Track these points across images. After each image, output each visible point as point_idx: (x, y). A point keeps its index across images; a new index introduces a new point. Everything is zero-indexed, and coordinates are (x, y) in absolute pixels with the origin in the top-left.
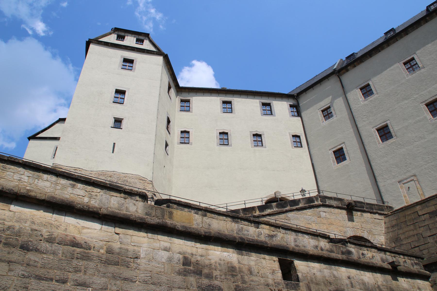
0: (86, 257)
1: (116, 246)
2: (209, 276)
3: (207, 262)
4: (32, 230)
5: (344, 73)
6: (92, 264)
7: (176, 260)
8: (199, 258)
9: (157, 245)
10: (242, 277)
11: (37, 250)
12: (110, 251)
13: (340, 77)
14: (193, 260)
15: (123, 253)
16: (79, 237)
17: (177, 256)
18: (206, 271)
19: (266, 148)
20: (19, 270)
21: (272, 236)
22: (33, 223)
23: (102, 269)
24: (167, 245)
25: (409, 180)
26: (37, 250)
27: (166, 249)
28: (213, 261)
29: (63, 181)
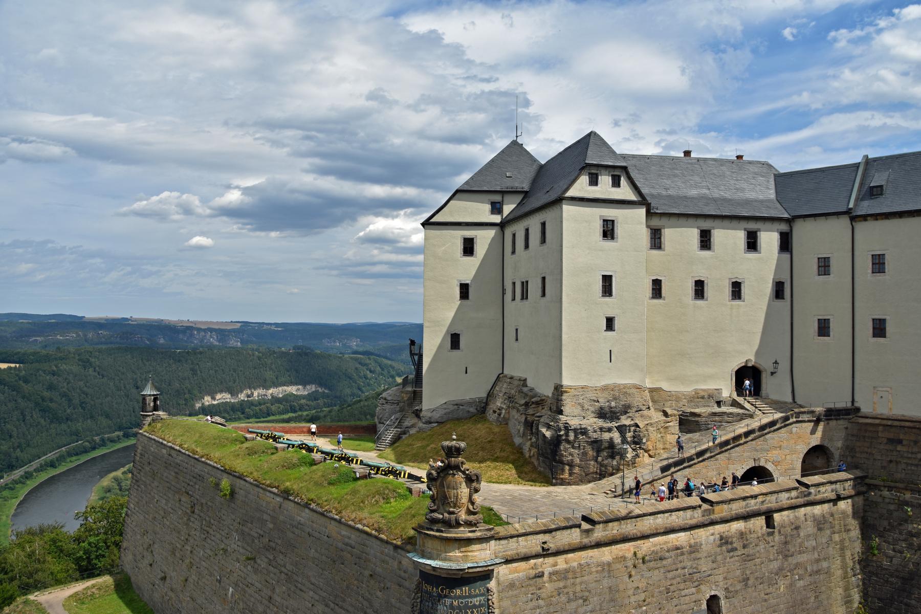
0: (682, 554)
1: (692, 541)
2: (731, 543)
3: (730, 534)
4: (661, 548)
5: (860, 221)
6: (685, 557)
7: (717, 539)
11: (665, 558)
12: (690, 546)
13: (853, 223)
14: (724, 536)
18: (730, 540)
19: (744, 301)
20: (662, 570)
22: (660, 544)
24: (712, 531)
25: (884, 389)
26: (665, 558)
27: (713, 534)
29: (666, 515)
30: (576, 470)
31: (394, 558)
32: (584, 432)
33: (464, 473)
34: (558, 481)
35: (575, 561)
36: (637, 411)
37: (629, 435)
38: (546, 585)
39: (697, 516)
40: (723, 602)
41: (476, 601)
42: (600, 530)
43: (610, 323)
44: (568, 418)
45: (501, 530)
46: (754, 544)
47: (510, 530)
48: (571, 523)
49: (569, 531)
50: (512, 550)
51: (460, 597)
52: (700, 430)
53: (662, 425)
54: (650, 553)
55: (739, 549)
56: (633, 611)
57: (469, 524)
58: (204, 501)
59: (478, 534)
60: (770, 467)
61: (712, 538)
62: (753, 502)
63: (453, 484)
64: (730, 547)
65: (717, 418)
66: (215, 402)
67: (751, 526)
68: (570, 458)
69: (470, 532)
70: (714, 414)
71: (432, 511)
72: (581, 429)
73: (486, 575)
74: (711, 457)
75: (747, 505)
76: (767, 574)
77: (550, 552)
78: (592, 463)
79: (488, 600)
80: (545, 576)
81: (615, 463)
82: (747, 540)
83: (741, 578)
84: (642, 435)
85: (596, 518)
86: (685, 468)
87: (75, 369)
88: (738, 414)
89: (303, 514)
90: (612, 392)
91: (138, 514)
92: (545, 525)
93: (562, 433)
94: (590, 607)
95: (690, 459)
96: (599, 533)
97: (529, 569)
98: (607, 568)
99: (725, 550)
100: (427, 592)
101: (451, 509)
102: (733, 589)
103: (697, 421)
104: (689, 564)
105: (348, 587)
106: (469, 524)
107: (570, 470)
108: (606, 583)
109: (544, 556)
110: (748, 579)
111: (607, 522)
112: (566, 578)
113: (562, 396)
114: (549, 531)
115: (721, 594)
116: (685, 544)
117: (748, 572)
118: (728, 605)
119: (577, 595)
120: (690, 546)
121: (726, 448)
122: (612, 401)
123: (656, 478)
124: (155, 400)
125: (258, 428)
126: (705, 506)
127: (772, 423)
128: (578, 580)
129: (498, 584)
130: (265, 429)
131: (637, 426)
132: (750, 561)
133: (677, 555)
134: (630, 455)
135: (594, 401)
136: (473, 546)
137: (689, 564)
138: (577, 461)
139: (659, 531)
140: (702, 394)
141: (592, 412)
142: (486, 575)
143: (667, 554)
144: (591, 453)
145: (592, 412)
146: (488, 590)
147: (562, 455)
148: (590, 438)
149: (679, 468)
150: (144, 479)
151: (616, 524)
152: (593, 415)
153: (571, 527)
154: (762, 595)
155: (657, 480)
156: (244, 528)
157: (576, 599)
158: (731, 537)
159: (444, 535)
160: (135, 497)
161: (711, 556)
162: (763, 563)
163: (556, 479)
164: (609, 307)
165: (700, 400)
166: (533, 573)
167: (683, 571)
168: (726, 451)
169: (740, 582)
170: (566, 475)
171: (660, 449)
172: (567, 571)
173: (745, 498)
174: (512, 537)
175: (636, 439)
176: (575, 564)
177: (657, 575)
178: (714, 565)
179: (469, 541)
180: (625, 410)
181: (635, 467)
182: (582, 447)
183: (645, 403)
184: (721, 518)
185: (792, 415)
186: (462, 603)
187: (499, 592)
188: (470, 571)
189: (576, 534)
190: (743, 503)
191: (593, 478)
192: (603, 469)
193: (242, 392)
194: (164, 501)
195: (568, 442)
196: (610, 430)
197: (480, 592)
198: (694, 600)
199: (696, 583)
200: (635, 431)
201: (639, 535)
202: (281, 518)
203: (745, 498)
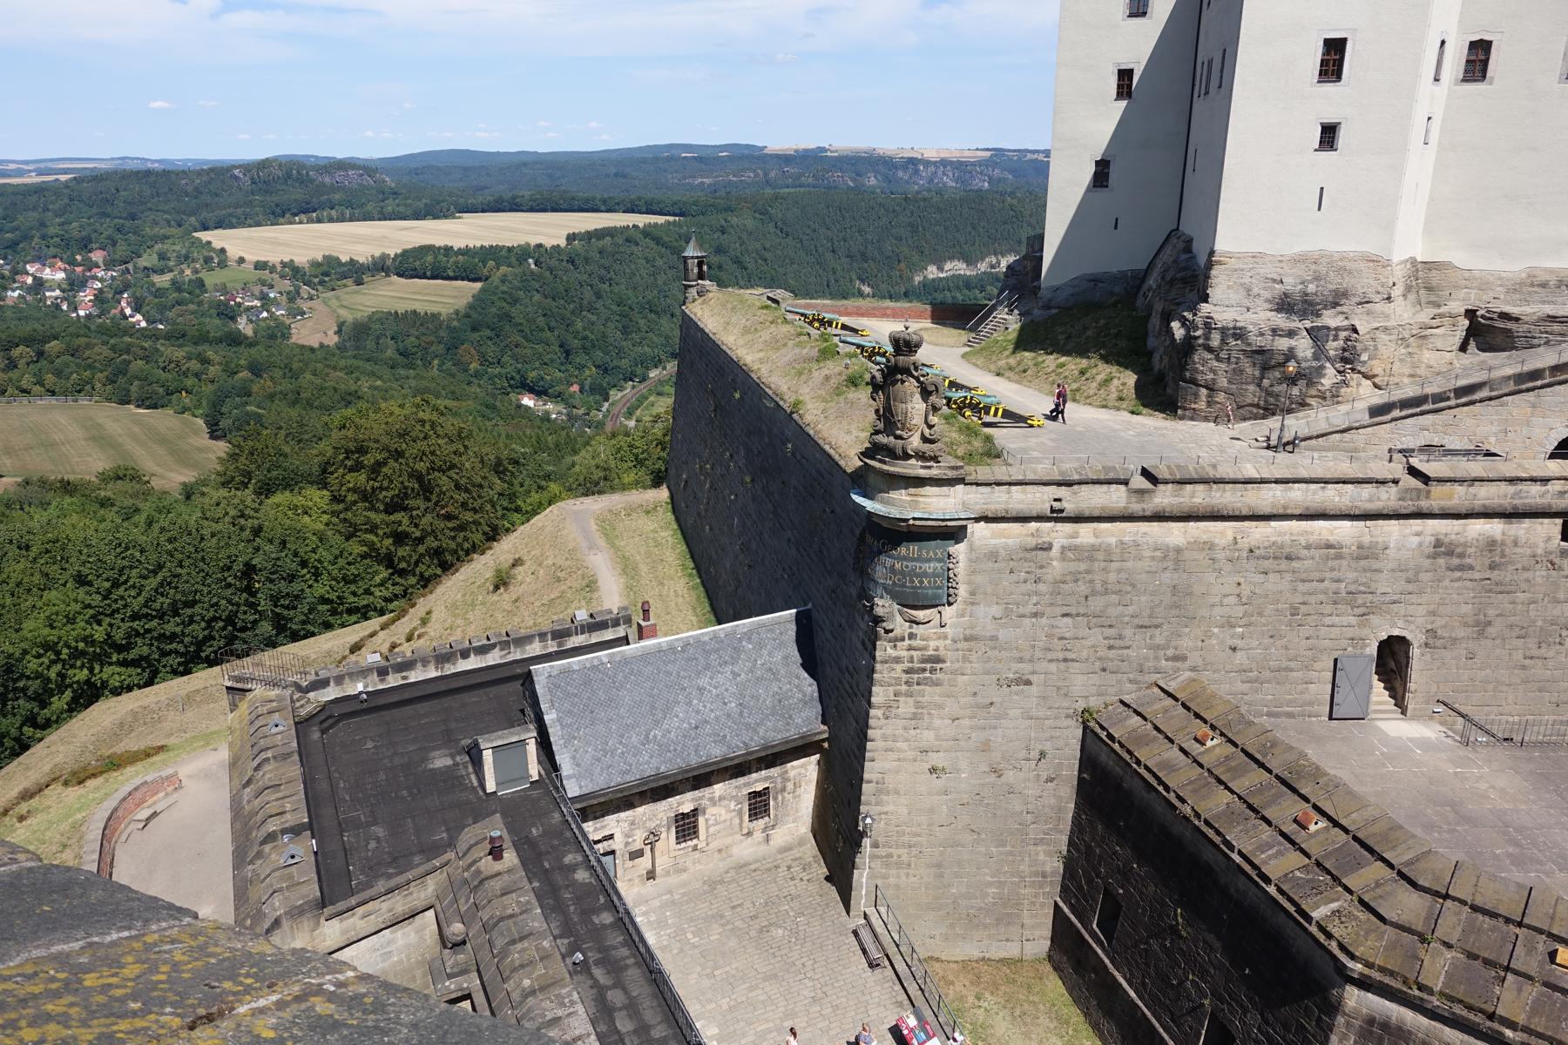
0: (1339, 557)
1: (1366, 540)
3: (1462, 540)
6: (1345, 563)
8: (1453, 537)
9: (1407, 531)
10: (1502, 551)
12: (1360, 547)
15: (1373, 545)
17: (1429, 540)
18: (1459, 550)
23: (1353, 564)
24: (1419, 529)
26: (1298, 558)
27: (1418, 534)
28: (1469, 539)
29: (1313, 486)
30: (1220, 397)
32: (1239, 333)
33: (917, 379)
34: (1188, 413)
35: (1113, 535)
36: (1360, 303)
37: (1333, 347)
38: (1055, 563)
39: (1387, 498)
40: (1415, 652)
41: (930, 567)
42: (1168, 493)
43: (1329, 135)
44: (1217, 308)
45: (999, 471)
46: (1519, 566)
47: (999, 471)
48: (1111, 475)
49: (1105, 487)
50: (998, 503)
51: (905, 558)
52: (1516, 348)
53: (1415, 332)
54: (1266, 544)
55: (1478, 568)
56: (1216, 630)
57: (921, 456)
59: (935, 472)
61: (1416, 540)
62: (1536, 489)
63: (901, 394)
64: (1456, 561)
65: (1556, 327)
66: (941, 275)
67: (1523, 532)
68: (1211, 376)
69: (922, 467)
71: (877, 432)
72: (1235, 328)
73: (954, 533)
74: (1490, 399)
75: (1515, 494)
76: (1540, 623)
77: (1064, 515)
78: (1252, 388)
79: (949, 569)
80: (1054, 550)
81: (1295, 391)
82: (1503, 555)
83: (1470, 620)
84: (1359, 346)
85: (1162, 472)
86: (1422, 413)
87: (750, 223)
90: (1313, 267)
92: (1062, 473)
93: (1198, 333)
94: (1131, 610)
96: (1164, 498)
97: (1027, 535)
98: (1174, 557)
99: (1443, 566)
101: (898, 432)
102: (1445, 635)
103: (1510, 330)
104: (1351, 576)
106: (921, 456)
107: (1209, 396)
108: (1167, 577)
109: (1057, 520)
110: (1489, 623)
112: (1091, 559)
114: (1069, 484)
115: (1415, 637)
116: (1347, 541)
117: (1491, 612)
118: (1428, 657)
119: (1109, 586)
120: (1360, 547)
121: (1531, 385)
122: (1310, 282)
123: (1357, 425)
124: (700, 264)
125: (801, 306)
126: (1414, 483)
129: (971, 549)
130: (807, 306)
131: (1355, 331)
132: (1501, 593)
134: (1329, 378)
135: (1274, 281)
136: (928, 488)
137: (1351, 576)
138: (1223, 382)
139: (1289, 512)
140: (1543, 277)
141: (1267, 301)
142: (954, 533)
143: (1305, 552)
144: (1250, 371)
145: (1267, 301)
146: (949, 556)
147: (1196, 371)
148: (1249, 344)
149: (1410, 411)
151: (1200, 487)
153: (1109, 482)
154: (1518, 656)
155: (1357, 428)
157: (1106, 592)
158: (1465, 545)
159: (885, 467)
161: (1407, 570)
162: (1534, 602)
163: (1185, 409)
164: (1331, 102)
165: (1536, 289)
166: (1032, 542)
167: (1335, 585)
168: (1528, 390)
169: (1466, 625)
170: (1202, 405)
171: (1402, 375)
172: (1095, 548)
173: (1512, 481)
174: (999, 484)
175: (1346, 354)
177: (1274, 583)
178: (1410, 587)
179: (920, 482)
180: (1336, 300)
181: (1338, 403)
182: (1233, 360)
183: (1381, 289)
184: (1442, 508)
186: (907, 567)
187: (971, 560)
188: (918, 523)
189: (1118, 494)
190: (1511, 489)
191: (1251, 412)
192: (1272, 400)
193: (983, 259)
195: (1209, 349)
196: (1291, 334)
197: (936, 554)
198: (1350, 636)
199: (1362, 610)
200: (1347, 339)
201: (1245, 512)
202: (775, 430)
203: (1512, 481)
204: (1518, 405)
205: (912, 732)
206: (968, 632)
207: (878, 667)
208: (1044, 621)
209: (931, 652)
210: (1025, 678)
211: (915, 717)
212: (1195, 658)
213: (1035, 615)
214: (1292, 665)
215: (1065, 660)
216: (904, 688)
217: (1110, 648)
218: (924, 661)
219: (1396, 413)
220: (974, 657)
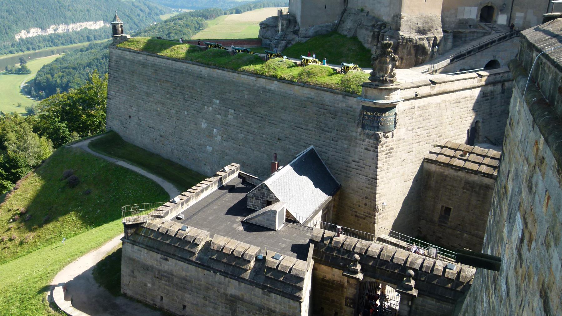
0: (468, 100)
16: (466, 95)
21: (502, 77)
30: (404, 61)
31: (343, 102)
32: (410, 40)
37: (432, 42)
58: (184, 84)
60: (499, 60)
62: (498, 76)
64: (486, 98)
65: (472, 35)
70: (471, 32)
73: (394, 107)
86: (461, 59)
88: (482, 33)
89: (273, 85)
91: (120, 97)
95: (464, 55)
96: (438, 88)
98: (438, 105)
100: (367, 115)
105: (309, 119)
111: (440, 83)
112: (423, 109)
113: (400, 20)
127: (504, 38)
128: (427, 111)
133: (466, 101)
143: (462, 100)
144: (413, 52)
150: (122, 76)
152: (414, 31)
156: (223, 96)
158: (488, 93)
160: (116, 87)
174: (405, 89)
176: (427, 103)
185: (515, 33)
194: (146, 87)
196: (423, 39)
204: (478, 55)
205: (387, 174)
206: (399, 138)
207: (379, 154)
208: (414, 131)
209: (391, 147)
210: (411, 150)
211: (388, 169)
212: (443, 136)
213: (412, 129)
214: (461, 133)
215: (419, 142)
216: (385, 160)
217: (427, 136)
218: (389, 150)
219: (455, 60)
220: (400, 146)
